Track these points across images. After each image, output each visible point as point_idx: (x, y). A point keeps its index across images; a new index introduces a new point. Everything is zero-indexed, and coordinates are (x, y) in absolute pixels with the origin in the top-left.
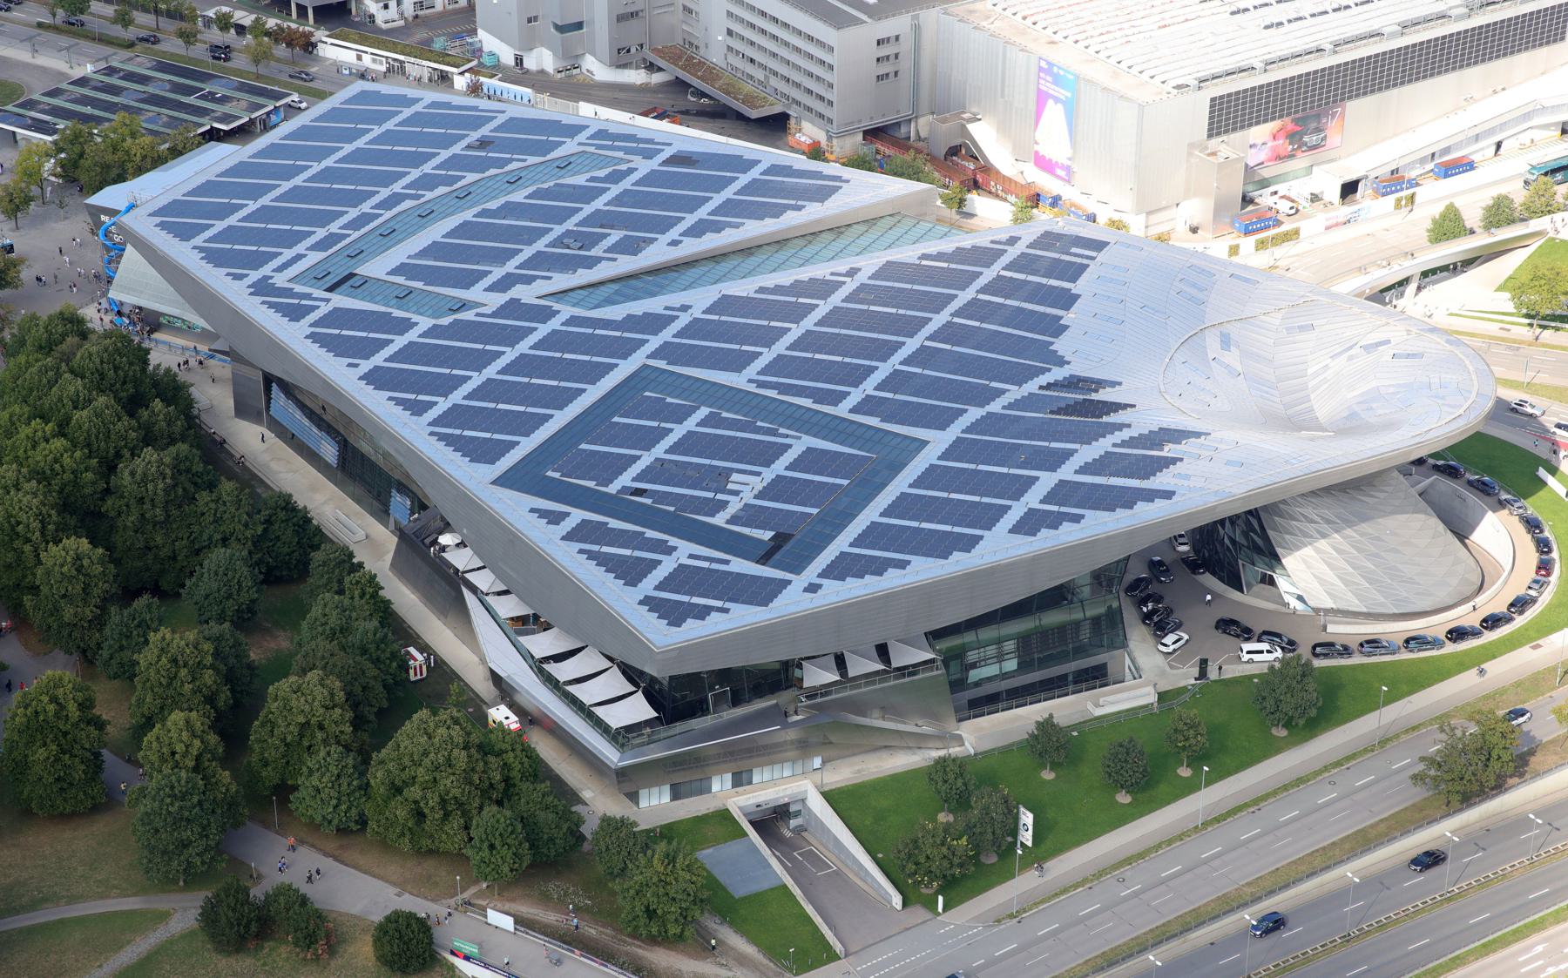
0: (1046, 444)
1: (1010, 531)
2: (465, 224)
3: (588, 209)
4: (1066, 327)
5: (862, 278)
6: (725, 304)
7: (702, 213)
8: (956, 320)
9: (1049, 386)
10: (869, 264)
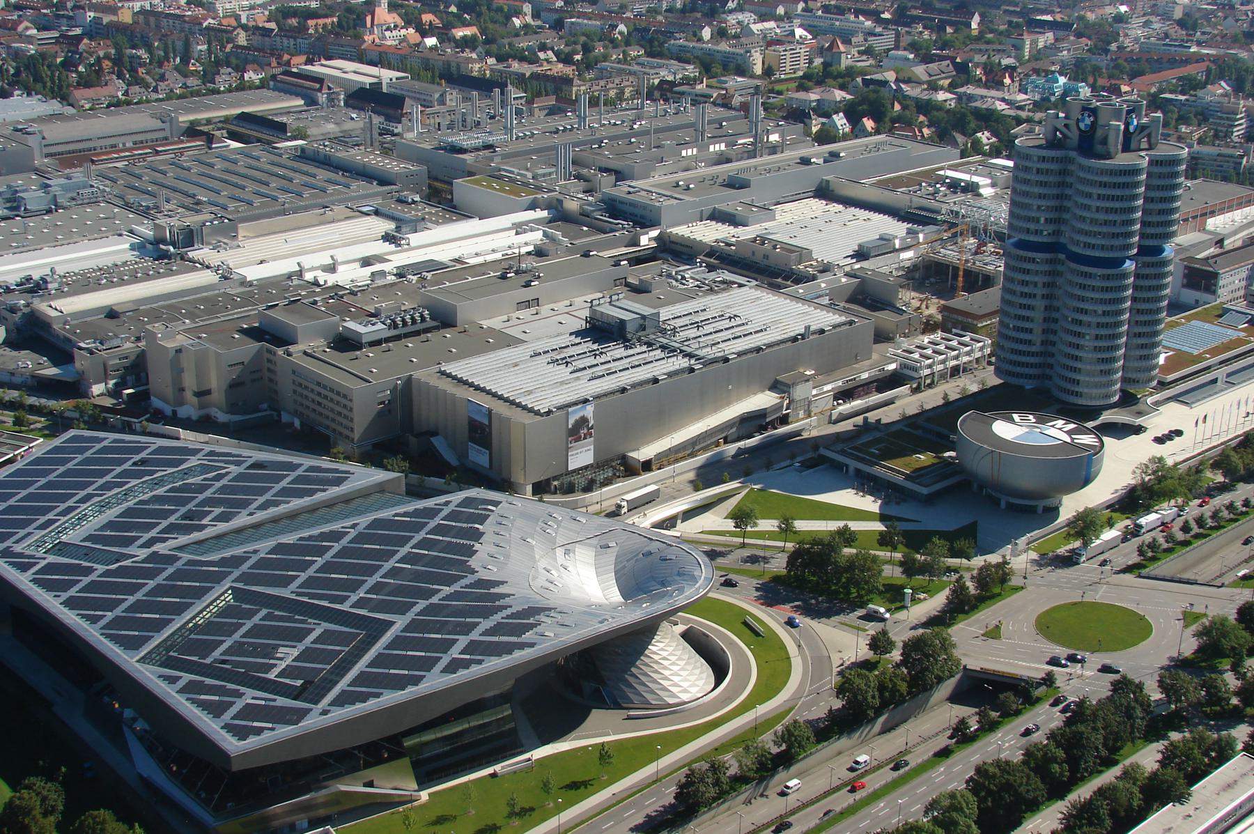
2: (129, 509)
3: (201, 497)
5: (360, 528)
6: (279, 548)
7: (268, 496)
8: (414, 550)
9: (466, 587)
10: (364, 521)
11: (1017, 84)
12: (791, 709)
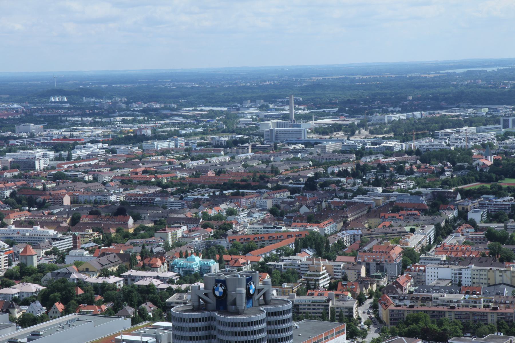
11: (166, 265)
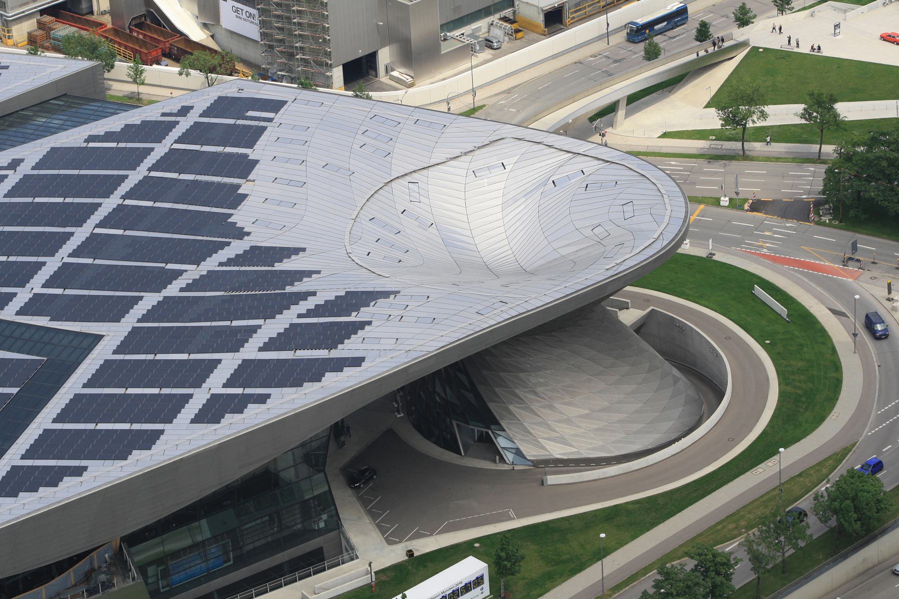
0: (227, 323)
1: (193, 421)
4: (245, 196)
5: (25, 169)
9: (229, 262)
12: (845, 452)
